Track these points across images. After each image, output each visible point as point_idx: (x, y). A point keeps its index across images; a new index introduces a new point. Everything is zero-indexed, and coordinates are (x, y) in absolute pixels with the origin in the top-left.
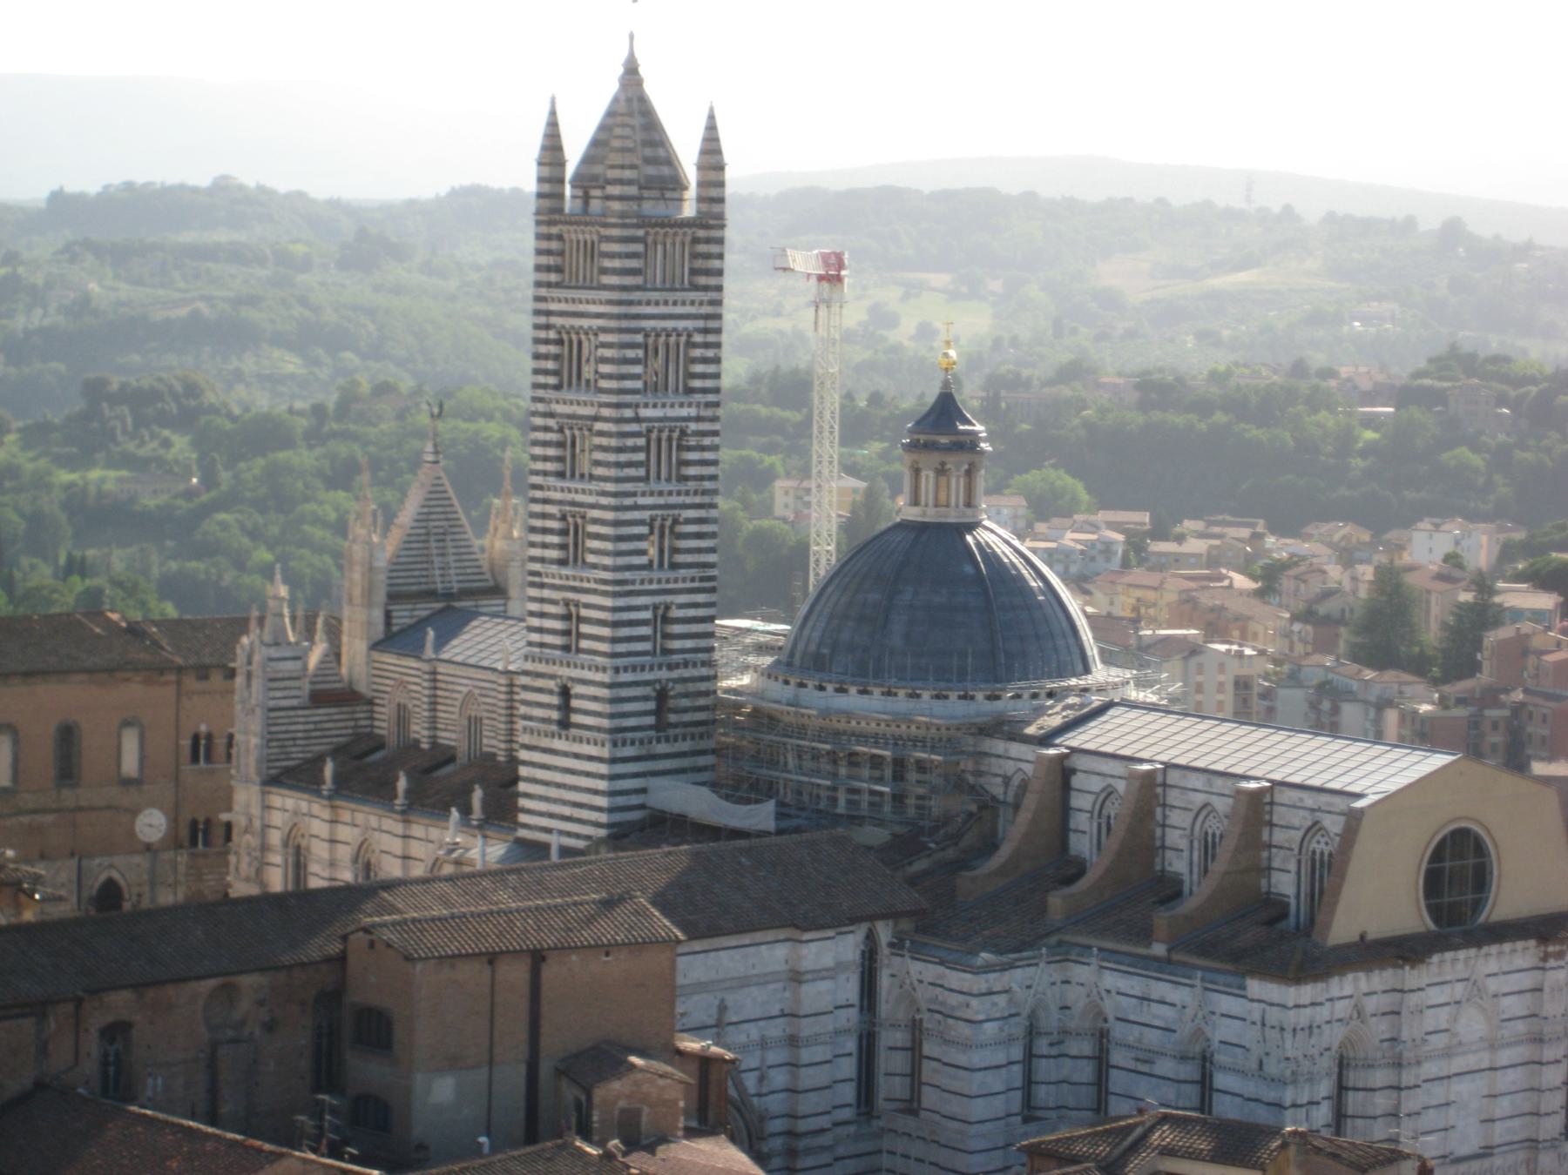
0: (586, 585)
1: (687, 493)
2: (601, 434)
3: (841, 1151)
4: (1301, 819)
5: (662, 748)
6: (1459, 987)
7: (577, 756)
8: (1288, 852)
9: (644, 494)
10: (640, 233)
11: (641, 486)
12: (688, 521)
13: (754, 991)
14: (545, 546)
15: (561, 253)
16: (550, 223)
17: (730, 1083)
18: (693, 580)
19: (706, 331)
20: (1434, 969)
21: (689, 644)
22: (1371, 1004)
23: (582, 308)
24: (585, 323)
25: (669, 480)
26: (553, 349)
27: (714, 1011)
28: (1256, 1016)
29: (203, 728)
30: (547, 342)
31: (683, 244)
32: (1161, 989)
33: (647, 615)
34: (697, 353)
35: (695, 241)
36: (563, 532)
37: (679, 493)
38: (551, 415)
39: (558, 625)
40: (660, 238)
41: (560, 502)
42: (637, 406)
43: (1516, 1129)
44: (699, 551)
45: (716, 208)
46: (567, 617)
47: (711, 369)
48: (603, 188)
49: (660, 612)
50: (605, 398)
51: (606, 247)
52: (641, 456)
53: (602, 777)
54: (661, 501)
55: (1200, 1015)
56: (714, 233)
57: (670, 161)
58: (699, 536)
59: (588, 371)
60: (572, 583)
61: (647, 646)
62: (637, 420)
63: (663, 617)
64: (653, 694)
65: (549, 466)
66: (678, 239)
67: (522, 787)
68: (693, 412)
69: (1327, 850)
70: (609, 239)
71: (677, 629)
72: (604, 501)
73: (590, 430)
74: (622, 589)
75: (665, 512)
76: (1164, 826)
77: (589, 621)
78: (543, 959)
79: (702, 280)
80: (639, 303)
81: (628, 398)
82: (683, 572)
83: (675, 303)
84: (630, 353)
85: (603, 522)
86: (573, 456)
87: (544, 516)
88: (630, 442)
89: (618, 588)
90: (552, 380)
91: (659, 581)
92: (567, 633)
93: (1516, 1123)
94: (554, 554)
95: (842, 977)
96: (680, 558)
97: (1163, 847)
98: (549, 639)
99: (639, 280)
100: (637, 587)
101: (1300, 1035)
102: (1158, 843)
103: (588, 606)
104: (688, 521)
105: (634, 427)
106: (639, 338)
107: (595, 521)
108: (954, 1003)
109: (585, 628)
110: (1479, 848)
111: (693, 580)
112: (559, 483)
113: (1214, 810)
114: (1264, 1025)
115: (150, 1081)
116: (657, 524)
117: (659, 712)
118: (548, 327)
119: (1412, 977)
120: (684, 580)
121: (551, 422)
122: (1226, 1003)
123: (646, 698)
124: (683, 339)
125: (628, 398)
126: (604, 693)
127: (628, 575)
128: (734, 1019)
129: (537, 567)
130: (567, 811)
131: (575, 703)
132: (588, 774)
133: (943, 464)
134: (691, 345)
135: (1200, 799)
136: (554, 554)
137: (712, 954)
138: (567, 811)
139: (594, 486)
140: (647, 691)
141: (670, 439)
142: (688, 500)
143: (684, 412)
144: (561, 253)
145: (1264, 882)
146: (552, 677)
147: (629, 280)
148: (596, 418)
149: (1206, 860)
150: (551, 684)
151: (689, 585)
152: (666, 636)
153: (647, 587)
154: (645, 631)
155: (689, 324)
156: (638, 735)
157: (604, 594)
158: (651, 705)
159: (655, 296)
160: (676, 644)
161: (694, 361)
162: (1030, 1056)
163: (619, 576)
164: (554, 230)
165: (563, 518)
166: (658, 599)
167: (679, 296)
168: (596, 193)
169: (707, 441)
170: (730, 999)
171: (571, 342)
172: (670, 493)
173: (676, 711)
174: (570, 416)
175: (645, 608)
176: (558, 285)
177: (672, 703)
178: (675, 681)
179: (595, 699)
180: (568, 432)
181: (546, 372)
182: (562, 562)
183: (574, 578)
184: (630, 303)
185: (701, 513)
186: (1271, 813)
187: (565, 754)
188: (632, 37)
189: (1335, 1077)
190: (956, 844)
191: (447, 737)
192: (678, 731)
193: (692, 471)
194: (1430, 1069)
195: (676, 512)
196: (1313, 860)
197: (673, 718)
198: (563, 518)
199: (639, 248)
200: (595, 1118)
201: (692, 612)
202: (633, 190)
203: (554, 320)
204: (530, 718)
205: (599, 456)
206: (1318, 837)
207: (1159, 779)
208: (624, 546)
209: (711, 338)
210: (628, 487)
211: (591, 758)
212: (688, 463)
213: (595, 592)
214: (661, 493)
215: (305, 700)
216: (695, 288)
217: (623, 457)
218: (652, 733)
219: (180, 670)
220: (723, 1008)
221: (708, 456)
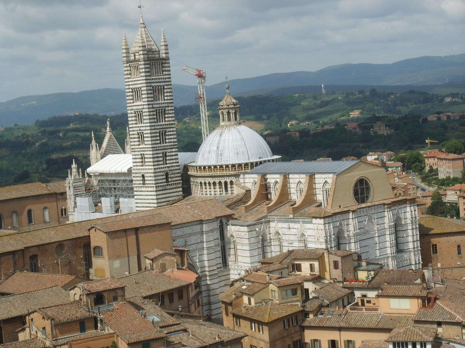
0: (145, 149)
3: (220, 275)
5: (168, 187)
7: (148, 191)
8: (320, 189)
9: (157, 126)
10: (149, 62)
11: (156, 124)
13: (193, 237)
14: (134, 142)
20: (358, 213)
27: (184, 242)
28: (316, 228)
29: (63, 207)
32: (292, 225)
33: (161, 155)
35: (162, 63)
36: (139, 138)
38: (133, 110)
39: (140, 160)
40: (154, 63)
41: (137, 130)
46: (142, 158)
48: (138, 53)
49: (164, 154)
55: (302, 229)
60: (142, 150)
62: (153, 108)
64: (165, 174)
65: (133, 122)
66: (158, 63)
68: (167, 105)
70: (141, 65)
72: (147, 128)
73: (142, 111)
74: (154, 149)
75: (163, 130)
76: (290, 188)
77: (147, 158)
78: (138, 230)
81: (150, 103)
85: (148, 133)
89: (153, 149)
92: (142, 162)
94: (137, 143)
95: (215, 232)
97: (290, 193)
98: (138, 164)
100: (158, 148)
102: (289, 193)
103: (146, 154)
104: (168, 132)
106: (151, 88)
107: (146, 134)
108: (243, 235)
109: (146, 160)
110: (367, 183)
112: (136, 126)
113: (301, 183)
114: (317, 229)
117: (167, 178)
121: (133, 112)
122: (309, 226)
123: (163, 175)
124: (162, 87)
126: (153, 175)
127: (155, 146)
128: (189, 244)
129: (133, 147)
130: (147, 205)
131: (146, 178)
132: (151, 195)
133: (229, 111)
135: (297, 180)
136: (137, 143)
137: (182, 228)
138: (147, 205)
140: (163, 173)
141: (162, 112)
145: (315, 198)
146: (140, 173)
147: (147, 74)
148: (143, 109)
149: (301, 193)
151: (170, 147)
153: (160, 148)
157: (150, 151)
163: (153, 146)
166: (163, 151)
167: (160, 77)
170: (188, 239)
171: (135, 91)
174: (137, 109)
175: (160, 153)
179: (151, 176)
182: (139, 145)
186: (315, 181)
187: (145, 191)
189: (337, 241)
190: (241, 200)
195: (165, 130)
196: (326, 190)
198: (138, 134)
200: (154, 266)
202: (146, 52)
204: (136, 184)
206: (327, 184)
210: (153, 124)
211: (151, 191)
218: (166, 184)
219: (56, 194)
220: (186, 242)
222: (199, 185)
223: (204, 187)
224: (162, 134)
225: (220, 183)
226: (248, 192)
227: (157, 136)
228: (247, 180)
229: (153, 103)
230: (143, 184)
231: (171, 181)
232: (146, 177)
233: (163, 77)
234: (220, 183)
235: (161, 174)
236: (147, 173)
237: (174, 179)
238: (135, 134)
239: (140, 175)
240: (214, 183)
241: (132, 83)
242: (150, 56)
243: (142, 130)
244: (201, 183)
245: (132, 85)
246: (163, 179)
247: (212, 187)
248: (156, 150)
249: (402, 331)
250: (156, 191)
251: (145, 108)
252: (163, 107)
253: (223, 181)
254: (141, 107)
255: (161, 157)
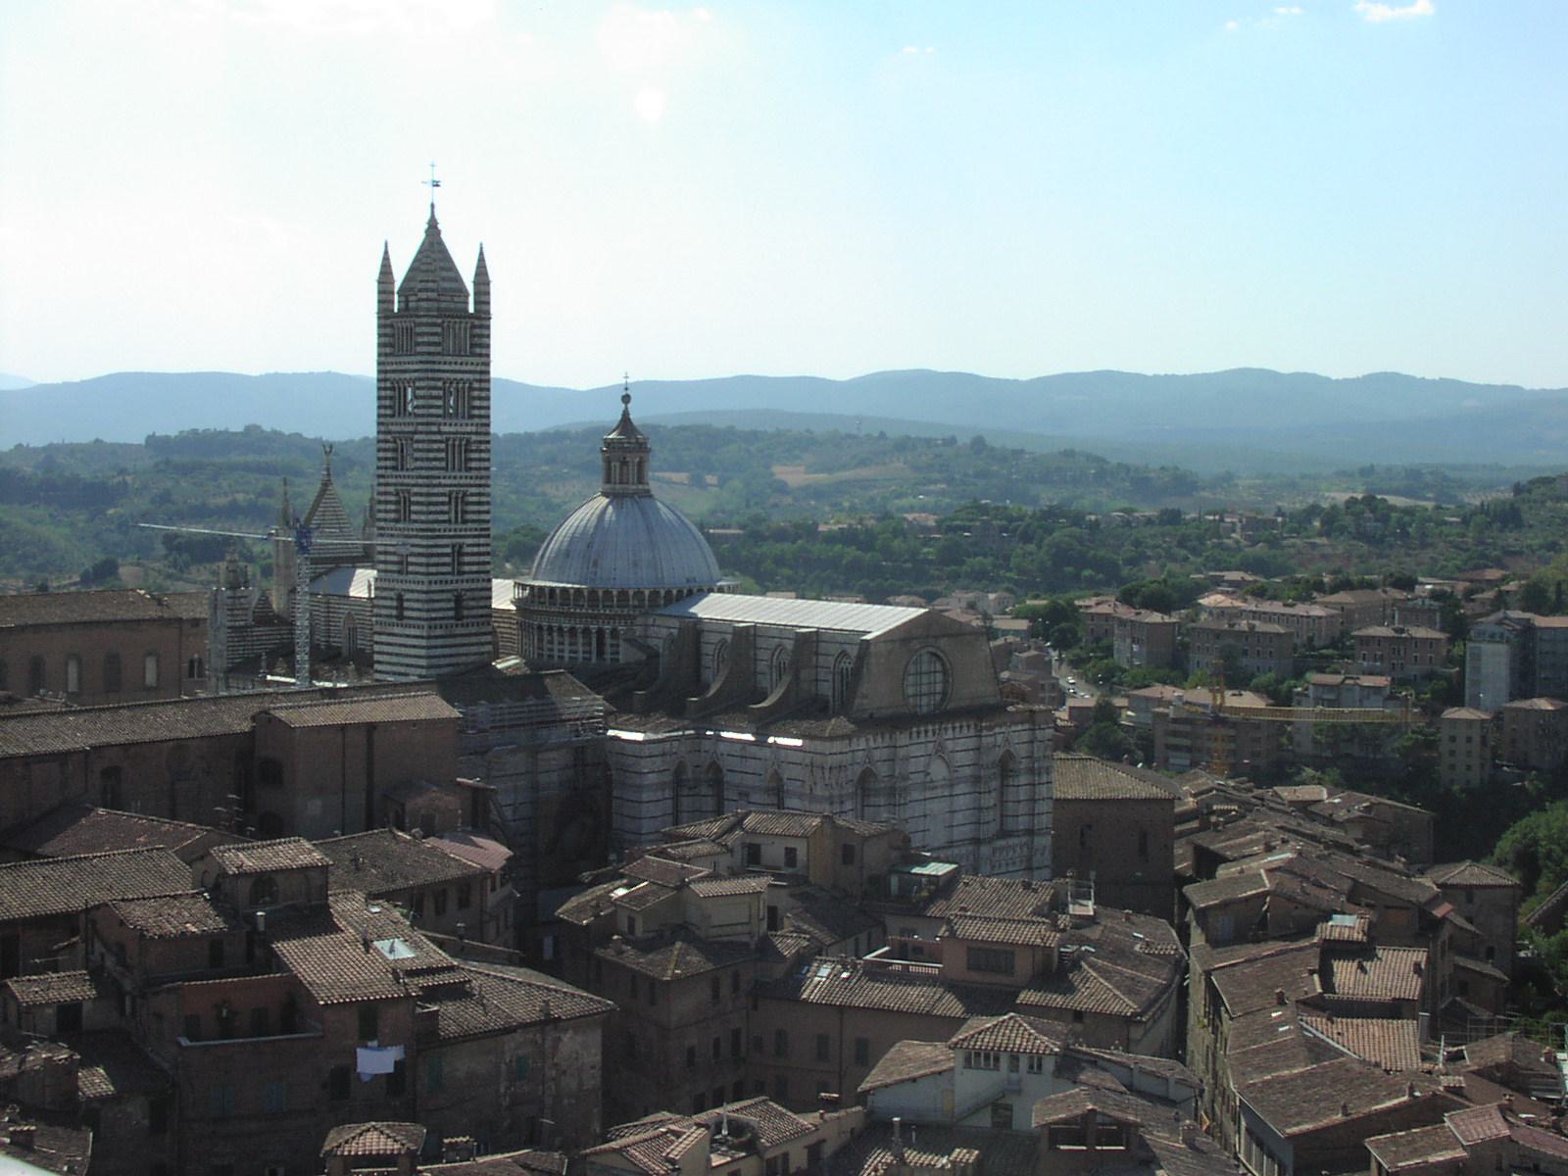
0: (411, 533)
1: (471, 478)
2: (418, 441)
4: (835, 649)
5: (460, 630)
6: (931, 745)
7: (408, 636)
9: (444, 478)
10: (439, 321)
11: (442, 473)
12: (472, 495)
14: (386, 511)
15: (393, 336)
16: (386, 318)
17: (491, 804)
18: (476, 530)
19: (481, 381)
21: (475, 568)
22: (877, 754)
23: (406, 367)
24: (407, 376)
25: (460, 470)
26: (389, 393)
28: (808, 761)
29: (196, 656)
30: (385, 389)
31: (465, 329)
33: (449, 550)
34: (476, 393)
35: (473, 327)
36: (397, 503)
37: (466, 477)
38: (389, 433)
41: (395, 485)
42: (440, 424)
43: (966, 832)
44: (479, 512)
45: (484, 307)
47: (484, 404)
49: (456, 549)
50: (420, 420)
51: (418, 330)
52: (443, 455)
53: (423, 647)
54: (456, 482)
56: (484, 323)
57: (458, 279)
58: (479, 503)
59: (410, 409)
61: (449, 569)
62: (439, 432)
63: (458, 552)
64: (453, 598)
65: (389, 463)
67: (377, 667)
68: (474, 429)
69: (850, 667)
71: (467, 559)
79: (478, 350)
80: (440, 363)
81: (434, 420)
82: (470, 525)
83: (461, 364)
84: (435, 393)
86: (402, 457)
87: (386, 493)
88: (435, 446)
90: (389, 412)
91: (455, 530)
93: (968, 827)
94: (392, 516)
96: (469, 517)
99: (439, 349)
100: (442, 533)
101: (834, 771)
104: (472, 495)
105: (438, 437)
106: (440, 384)
107: (416, 494)
111: (476, 530)
112: (395, 473)
113: (784, 648)
115: (133, 804)
116: (454, 495)
118: (386, 380)
119: (902, 739)
120: (471, 530)
121: (389, 437)
123: (449, 600)
125: (434, 420)
127: (436, 526)
131: (406, 604)
132: (414, 646)
134: (471, 389)
139: (414, 473)
140: (449, 596)
141: (460, 445)
142: (472, 482)
143: (469, 429)
144: (393, 336)
145: (813, 689)
146: (392, 590)
148: (415, 433)
150: (392, 594)
152: (461, 564)
153: (447, 533)
154: (447, 560)
155: (471, 376)
156: (444, 622)
158: (452, 605)
159: (449, 359)
160: (466, 568)
161: (474, 398)
162: (676, 798)
164: (388, 322)
165: (397, 494)
167: (464, 359)
168: (412, 298)
169: (483, 447)
172: (461, 477)
173: (469, 608)
174: (399, 433)
175: (447, 546)
176: (391, 354)
177: (465, 603)
178: (467, 590)
179: (417, 601)
180: (398, 442)
181: (385, 407)
182: (397, 521)
183: (404, 529)
184: (434, 362)
185: (481, 490)
186: (817, 646)
188: (433, 206)
191: (336, 641)
192: (469, 620)
193: (474, 464)
194: (916, 795)
195: (465, 489)
197: (465, 613)
199: (439, 330)
201: (476, 549)
203: (389, 376)
204: (380, 616)
205: (417, 455)
207: (752, 632)
208: (432, 508)
209: (484, 385)
212: (471, 460)
213: (416, 537)
214: (455, 478)
215: (251, 621)
216: (473, 355)
217: (431, 455)
221: (483, 455)
222: (535, 633)
223: (546, 637)
224: (457, 498)
225: (586, 632)
226: (653, 655)
227: (443, 503)
228: (652, 631)
229: (440, 420)
230: (396, 617)
231: (468, 617)
232: (408, 600)
233: (471, 359)
234: (586, 632)
235: (444, 596)
236: (412, 591)
237: (474, 612)
238: (390, 494)
239: (392, 594)
240: (572, 631)
241: (394, 367)
242: (443, 305)
243: (408, 485)
244: (540, 628)
245: (394, 371)
246: (449, 609)
247: (567, 641)
248: (438, 537)
249: (988, 1025)
250: (429, 637)
251: (421, 433)
252: (464, 433)
253: (594, 628)
254: (411, 428)
255: (447, 555)
